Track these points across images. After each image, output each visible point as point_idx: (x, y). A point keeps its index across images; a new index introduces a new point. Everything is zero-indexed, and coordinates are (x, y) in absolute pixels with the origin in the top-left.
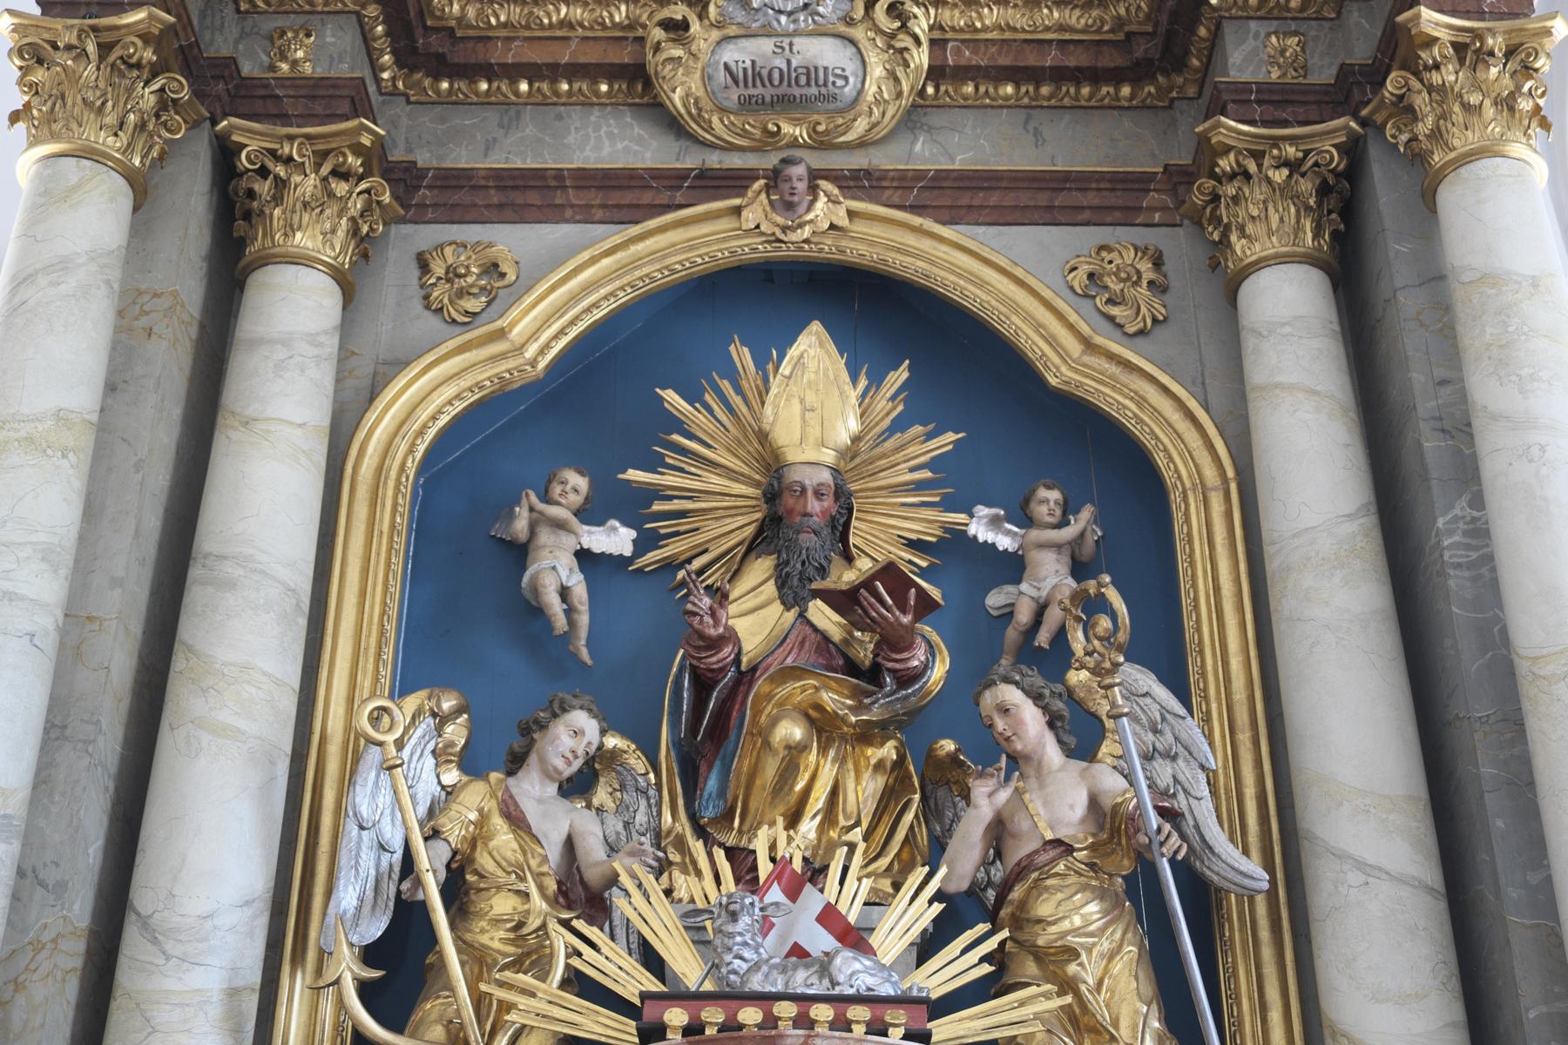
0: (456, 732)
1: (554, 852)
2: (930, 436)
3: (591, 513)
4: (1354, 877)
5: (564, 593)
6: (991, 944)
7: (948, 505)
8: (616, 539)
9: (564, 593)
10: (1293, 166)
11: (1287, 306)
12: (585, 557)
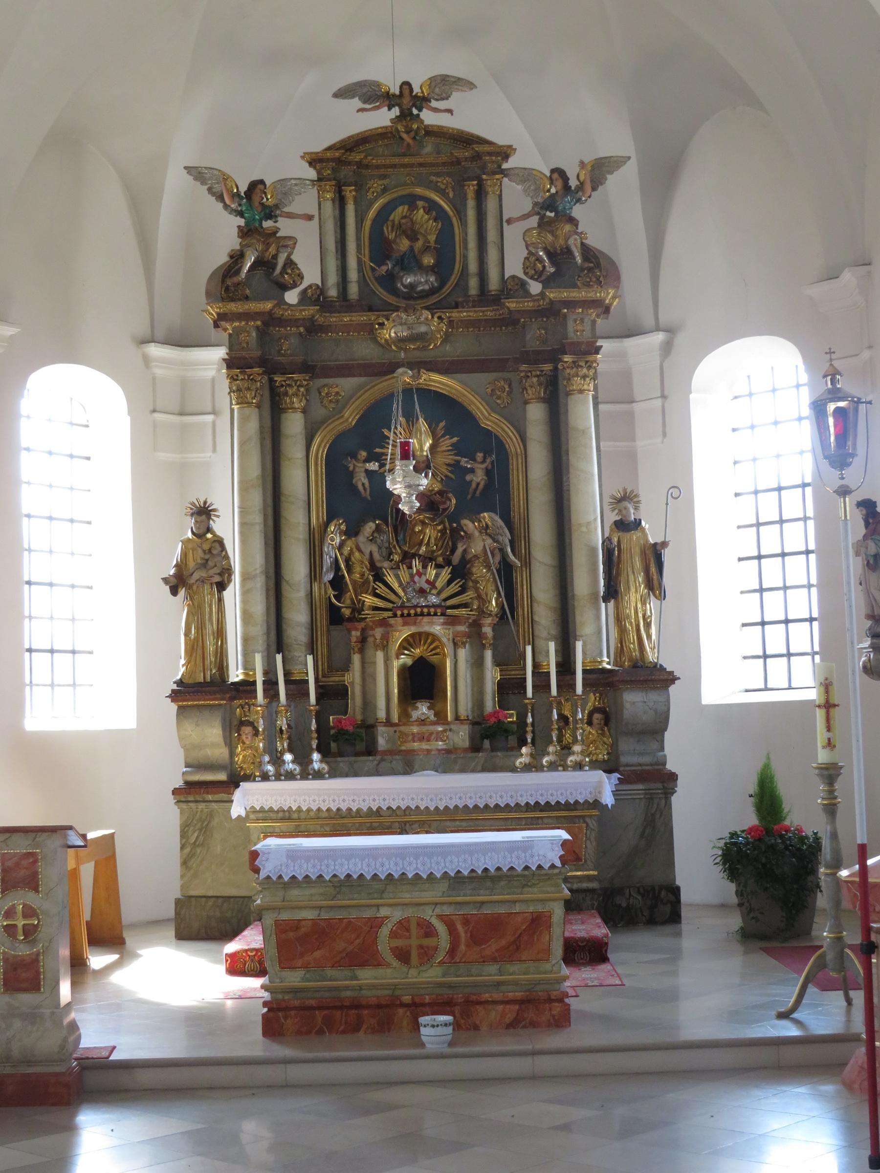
0: (343, 527)
1: (367, 556)
2: (451, 438)
3: (368, 460)
4: (538, 564)
5: (363, 484)
6: (461, 583)
7: (456, 455)
9: (363, 484)
10: (538, 376)
11: (536, 413)
12: (367, 471)
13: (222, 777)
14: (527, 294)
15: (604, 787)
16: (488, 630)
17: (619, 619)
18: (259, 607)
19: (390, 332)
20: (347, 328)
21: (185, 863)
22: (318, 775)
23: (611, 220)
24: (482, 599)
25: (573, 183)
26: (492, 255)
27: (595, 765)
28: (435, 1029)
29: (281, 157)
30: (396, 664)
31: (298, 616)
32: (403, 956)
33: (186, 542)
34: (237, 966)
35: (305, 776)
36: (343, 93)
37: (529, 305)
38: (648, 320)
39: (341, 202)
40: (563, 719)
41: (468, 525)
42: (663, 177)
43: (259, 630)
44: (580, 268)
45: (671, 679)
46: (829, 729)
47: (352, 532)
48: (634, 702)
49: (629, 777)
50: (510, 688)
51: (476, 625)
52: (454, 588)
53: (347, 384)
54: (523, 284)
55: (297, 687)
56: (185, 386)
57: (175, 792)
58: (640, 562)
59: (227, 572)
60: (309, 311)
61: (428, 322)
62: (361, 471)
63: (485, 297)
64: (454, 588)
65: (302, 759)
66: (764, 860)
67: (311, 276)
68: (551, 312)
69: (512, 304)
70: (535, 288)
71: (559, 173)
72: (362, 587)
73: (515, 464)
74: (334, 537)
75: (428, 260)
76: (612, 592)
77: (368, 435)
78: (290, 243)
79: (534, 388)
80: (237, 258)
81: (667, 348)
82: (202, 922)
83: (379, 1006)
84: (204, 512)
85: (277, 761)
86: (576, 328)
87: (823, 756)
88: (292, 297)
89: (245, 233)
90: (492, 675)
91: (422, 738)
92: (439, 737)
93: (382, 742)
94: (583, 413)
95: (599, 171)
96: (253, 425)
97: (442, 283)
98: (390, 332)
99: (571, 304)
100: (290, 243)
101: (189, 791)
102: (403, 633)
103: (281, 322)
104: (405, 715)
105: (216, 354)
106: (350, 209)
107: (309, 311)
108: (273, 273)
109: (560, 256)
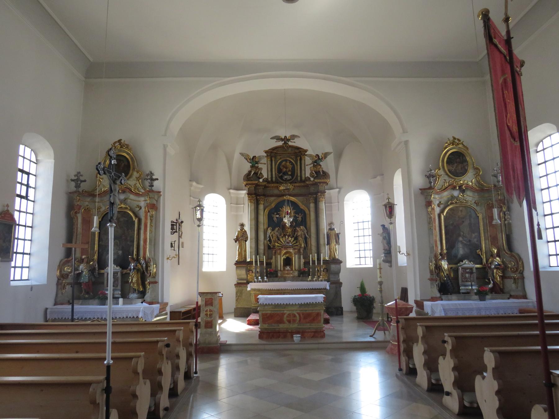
8: (278, 216)
11: (312, 205)
12: (277, 217)
13: (245, 282)
14: (310, 180)
15: (327, 285)
16: (302, 251)
17: (330, 249)
18: (254, 246)
19: (282, 188)
20: (273, 187)
21: (237, 300)
22: (266, 282)
23: (328, 165)
24: (301, 245)
25: (320, 157)
26: (303, 172)
27: (325, 280)
28: (297, 338)
29: (259, 151)
30: (282, 258)
31: (261, 247)
32: (289, 321)
33: (238, 231)
34: (250, 323)
35: (263, 282)
36: (272, 138)
37: (311, 183)
38: (335, 186)
39: (271, 161)
40: (318, 270)
41: (297, 228)
42: (339, 156)
43: (253, 250)
44: (321, 175)
45: (341, 262)
47: (273, 230)
48: (333, 267)
49: (332, 283)
50: (307, 263)
51: (299, 250)
52: (295, 242)
53: (273, 198)
54: (309, 178)
55: (262, 263)
56: (237, 198)
57: (235, 285)
58: (335, 237)
59: (247, 238)
60: (265, 183)
61: (290, 186)
62: (275, 217)
63: (301, 181)
64: (295, 242)
65: (262, 278)
67: (265, 176)
68: (316, 184)
69: (307, 183)
70: (312, 179)
71: (317, 155)
72: (275, 242)
73: (308, 216)
74: (269, 231)
75: (290, 173)
76: (328, 243)
77: (277, 209)
78: (261, 169)
79: (312, 200)
80: (250, 172)
81: (339, 192)
82: (241, 313)
83: (284, 332)
84: (242, 225)
85: (257, 278)
86: (321, 188)
87: (379, 280)
88: (261, 180)
89: (252, 167)
90: (303, 261)
91: (288, 274)
92: (291, 274)
93: (279, 275)
94: (322, 205)
95: (326, 155)
96: (253, 207)
97: (293, 178)
98: (282, 188)
99: (320, 183)
100: (261, 169)
101: (238, 285)
102: (284, 252)
103: (259, 186)
104: (284, 269)
105: (244, 192)
106: (273, 162)
107: (265, 183)
108: (258, 175)
109: (317, 173)
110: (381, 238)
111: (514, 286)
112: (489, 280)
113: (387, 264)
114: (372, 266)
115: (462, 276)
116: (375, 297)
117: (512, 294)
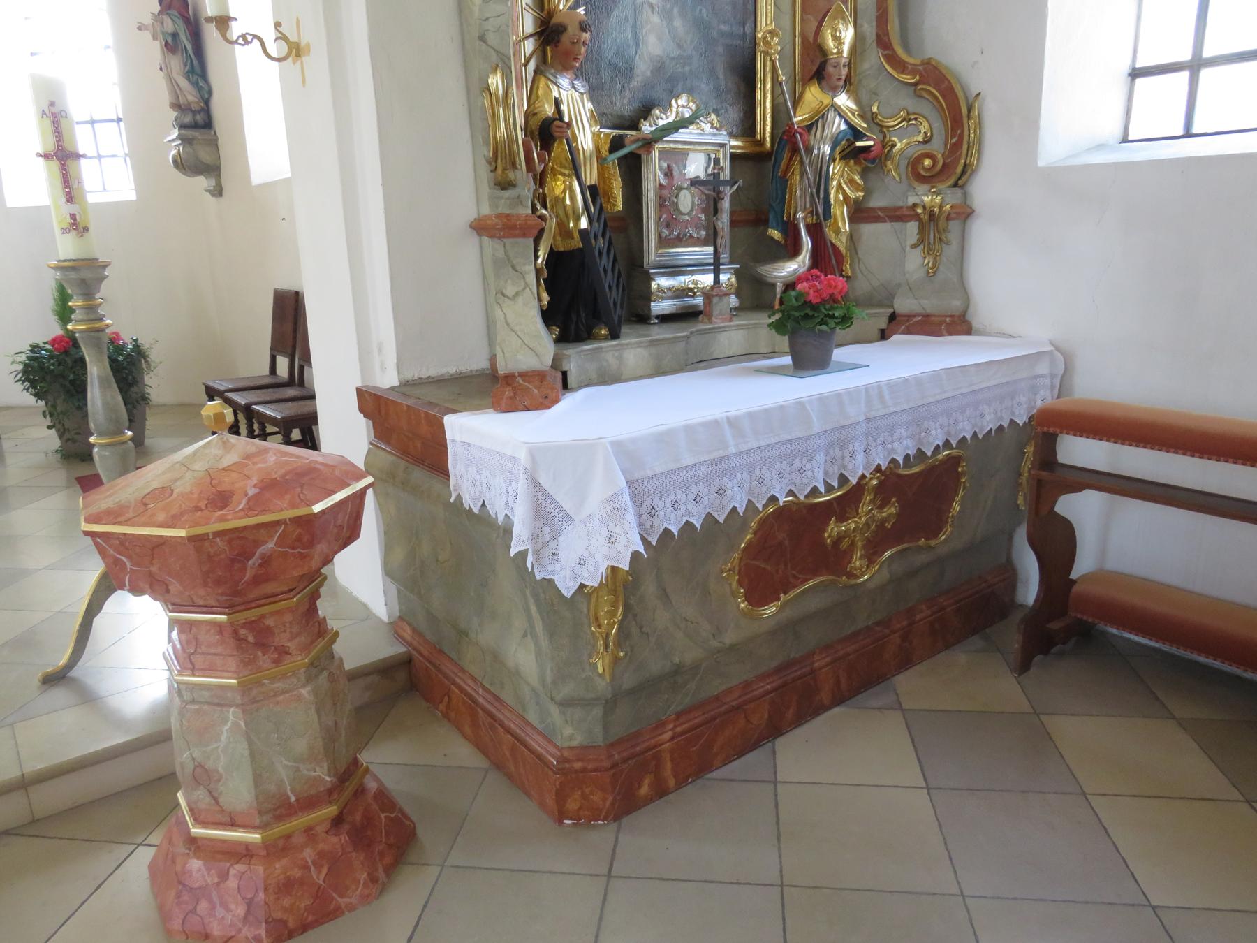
46: (70, 198)
66: (71, 377)
110: (155, 49)
111: (915, 261)
112: (791, 231)
113: (202, 182)
114: (131, 196)
115: (661, 202)
116: (145, 342)
117: (904, 305)
